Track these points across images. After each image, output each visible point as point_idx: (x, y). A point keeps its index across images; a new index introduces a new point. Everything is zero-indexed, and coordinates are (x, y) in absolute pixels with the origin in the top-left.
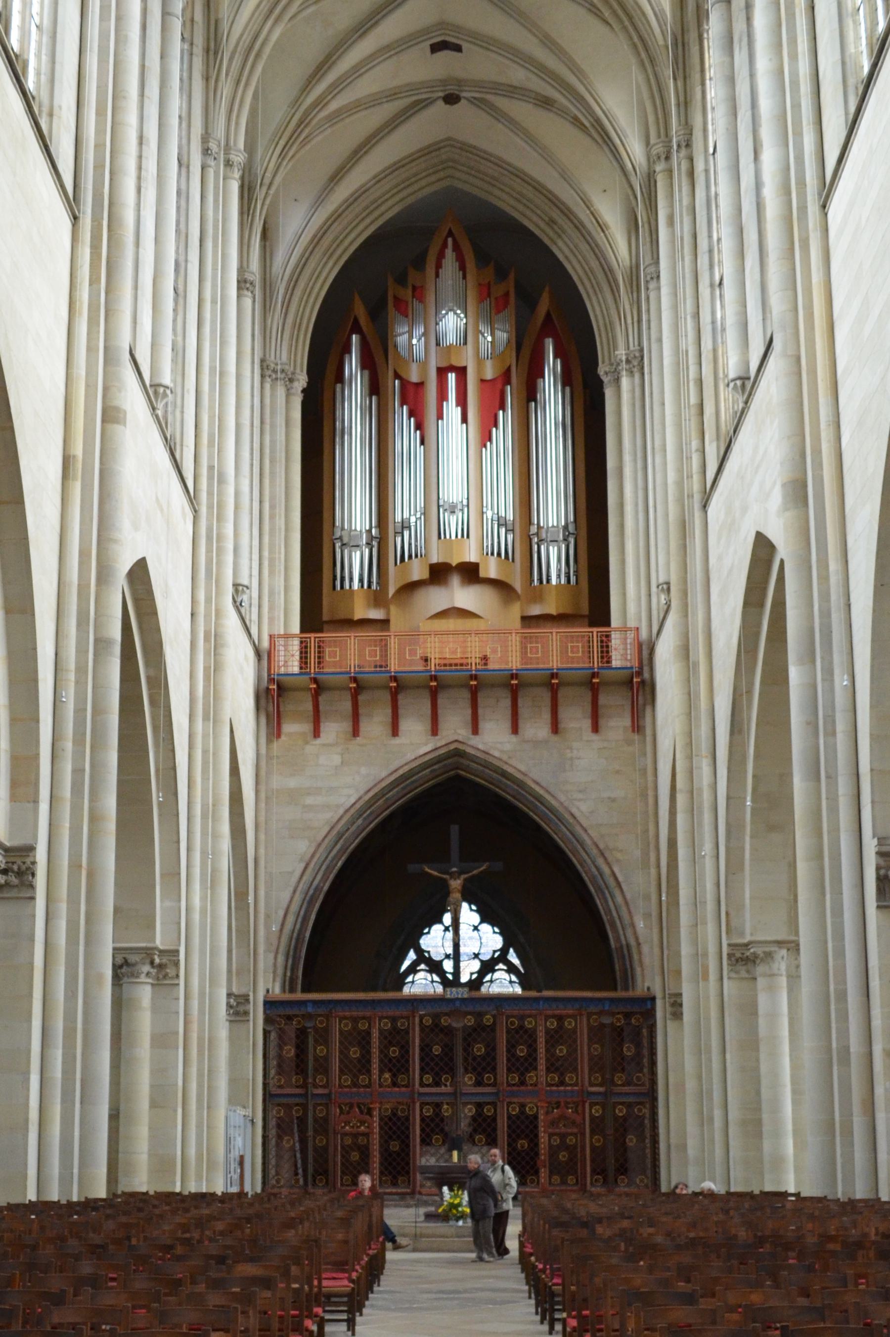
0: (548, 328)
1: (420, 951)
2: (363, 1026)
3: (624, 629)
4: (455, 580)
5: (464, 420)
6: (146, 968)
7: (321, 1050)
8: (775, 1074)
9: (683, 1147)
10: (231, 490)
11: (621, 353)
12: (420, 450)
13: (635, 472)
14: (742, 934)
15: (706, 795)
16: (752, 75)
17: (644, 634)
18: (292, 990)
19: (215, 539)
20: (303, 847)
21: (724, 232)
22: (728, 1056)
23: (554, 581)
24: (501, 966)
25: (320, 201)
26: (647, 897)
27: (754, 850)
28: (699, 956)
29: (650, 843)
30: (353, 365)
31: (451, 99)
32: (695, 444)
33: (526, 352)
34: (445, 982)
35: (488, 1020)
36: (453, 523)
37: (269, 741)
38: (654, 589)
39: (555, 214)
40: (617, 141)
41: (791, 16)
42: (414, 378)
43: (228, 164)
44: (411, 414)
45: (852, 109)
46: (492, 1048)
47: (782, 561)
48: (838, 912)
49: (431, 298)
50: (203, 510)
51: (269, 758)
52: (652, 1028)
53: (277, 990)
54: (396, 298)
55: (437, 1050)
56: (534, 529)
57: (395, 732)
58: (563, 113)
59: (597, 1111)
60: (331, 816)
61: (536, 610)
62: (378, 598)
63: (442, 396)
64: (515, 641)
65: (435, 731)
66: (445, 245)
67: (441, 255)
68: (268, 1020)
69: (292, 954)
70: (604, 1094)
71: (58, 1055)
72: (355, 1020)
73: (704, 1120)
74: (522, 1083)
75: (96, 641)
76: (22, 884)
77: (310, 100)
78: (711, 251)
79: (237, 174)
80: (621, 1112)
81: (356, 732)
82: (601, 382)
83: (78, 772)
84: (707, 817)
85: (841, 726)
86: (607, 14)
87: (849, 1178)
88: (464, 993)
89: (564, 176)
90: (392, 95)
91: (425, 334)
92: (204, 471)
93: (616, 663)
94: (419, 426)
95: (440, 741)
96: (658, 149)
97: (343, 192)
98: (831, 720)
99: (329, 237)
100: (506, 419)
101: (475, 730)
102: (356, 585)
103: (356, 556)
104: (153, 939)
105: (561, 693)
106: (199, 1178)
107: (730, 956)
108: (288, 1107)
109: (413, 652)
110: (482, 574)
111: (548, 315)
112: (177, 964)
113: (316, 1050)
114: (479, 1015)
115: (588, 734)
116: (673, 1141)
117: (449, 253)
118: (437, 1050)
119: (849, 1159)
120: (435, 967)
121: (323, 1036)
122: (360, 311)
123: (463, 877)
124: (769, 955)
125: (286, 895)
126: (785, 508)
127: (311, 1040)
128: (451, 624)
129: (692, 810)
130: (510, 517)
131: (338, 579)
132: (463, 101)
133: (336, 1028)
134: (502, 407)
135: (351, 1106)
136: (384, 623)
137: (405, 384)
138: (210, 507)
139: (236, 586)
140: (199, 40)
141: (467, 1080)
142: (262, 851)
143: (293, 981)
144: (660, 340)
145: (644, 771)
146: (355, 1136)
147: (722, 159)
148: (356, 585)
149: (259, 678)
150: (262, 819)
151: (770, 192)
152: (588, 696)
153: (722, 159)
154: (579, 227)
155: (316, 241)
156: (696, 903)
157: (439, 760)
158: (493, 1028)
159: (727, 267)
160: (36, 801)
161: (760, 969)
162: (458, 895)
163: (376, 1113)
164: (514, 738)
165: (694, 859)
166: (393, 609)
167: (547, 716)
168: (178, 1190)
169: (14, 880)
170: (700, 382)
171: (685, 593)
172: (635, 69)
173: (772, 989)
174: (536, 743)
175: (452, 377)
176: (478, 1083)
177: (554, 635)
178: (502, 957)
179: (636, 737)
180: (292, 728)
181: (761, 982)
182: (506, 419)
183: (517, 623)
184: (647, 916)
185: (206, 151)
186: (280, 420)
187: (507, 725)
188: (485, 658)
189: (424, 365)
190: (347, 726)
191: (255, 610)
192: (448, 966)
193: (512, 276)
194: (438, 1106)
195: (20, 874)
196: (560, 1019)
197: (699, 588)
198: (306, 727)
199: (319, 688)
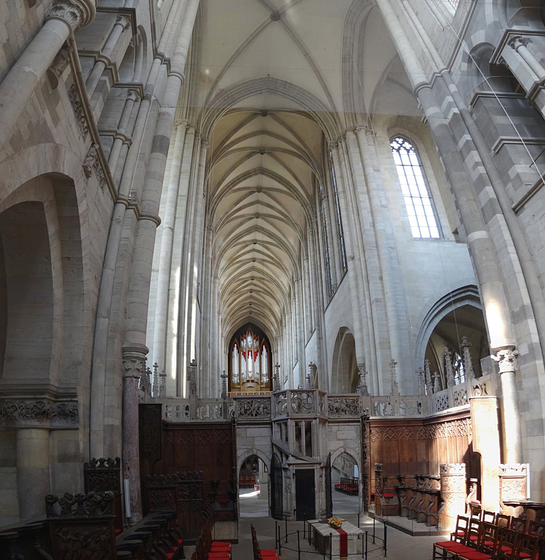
25: (231, 327)
33: (261, 347)
61: (262, 386)
63: (249, 355)
67: (248, 333)
100: (258, 357)
154: (269, 330)
175: (250, 352)
189: (246, 349)
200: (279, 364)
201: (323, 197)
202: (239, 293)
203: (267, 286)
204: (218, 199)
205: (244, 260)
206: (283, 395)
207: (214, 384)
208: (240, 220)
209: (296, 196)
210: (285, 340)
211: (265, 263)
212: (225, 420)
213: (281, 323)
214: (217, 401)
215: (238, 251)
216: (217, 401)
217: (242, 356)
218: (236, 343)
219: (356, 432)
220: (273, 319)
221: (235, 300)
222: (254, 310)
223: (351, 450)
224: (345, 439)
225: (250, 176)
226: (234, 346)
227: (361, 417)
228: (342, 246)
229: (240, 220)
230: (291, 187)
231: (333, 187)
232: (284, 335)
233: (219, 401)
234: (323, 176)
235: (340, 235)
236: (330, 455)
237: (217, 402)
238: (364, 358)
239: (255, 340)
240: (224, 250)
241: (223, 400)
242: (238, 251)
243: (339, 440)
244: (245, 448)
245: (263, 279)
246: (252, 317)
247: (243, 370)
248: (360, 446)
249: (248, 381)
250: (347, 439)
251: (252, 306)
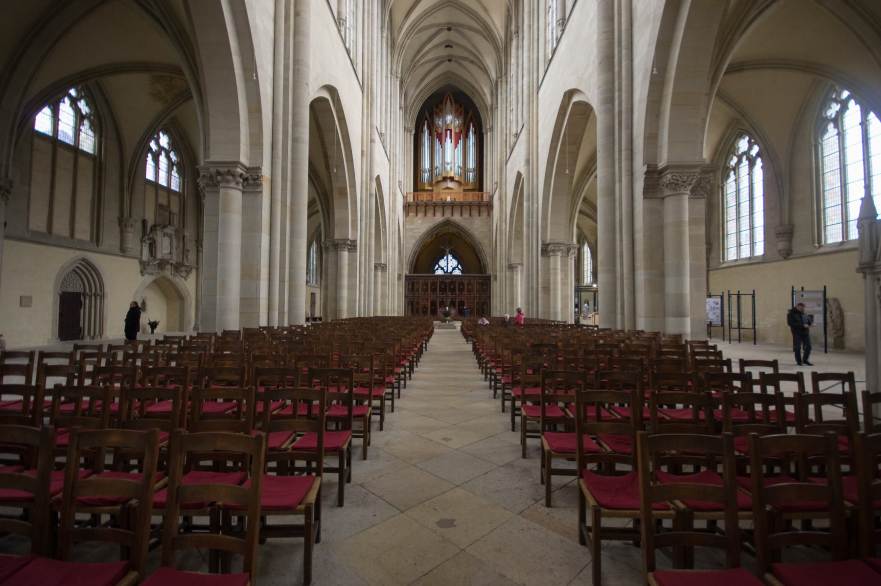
0: (471, 120)
1: (439, 265)
2: (427, 281)
3: (487, 193)
4: (449, 181)
5: (451, 142)
6: (380, 268)
7: (417, 286)
8: (517, 292)
9: (496, 308)
10: (398, 159)
11: (488, 126)
12: (441, 149)
13: (490, 155)
14: (511, 262)
15: (504, 231)
16: (523, 57)
17: (491, 194)
18: (411, 273)
19: (394, 170)
20: (414, 241)
21: (514, 97)
22: (507, 289)
23: (471, 181)
24: (457, 268)
25: (418, 86)
26: (490, 254)
27: (514, 243)
28: (501, 267)
29: (491, 241)
30: (425, 128)
31: (450, 60)
32: (504, 149)
33: (466, 125)
34: (444, 272)
35: (454, 280)
36: (448, 167)
37: (406, 217)
38: (494, 183)
40: (489, 72)
41: (533, 42)
42: (440, 132)
43: (397, 77)
44: (439, 141)
45: (546, 67)
46: (455, 287)
47: (523, 178)
48: (532, 257)
49: (444, 112)
50: (392, 163)
51: (406, 221)
52: (490, 283)
53: (408, 273)
54: (436, 112)
55: (443, 287)
56: (466, 169)
57: (434, 215)
58: (476, 65)
59: (478, 300)
60: (420, 234)
61: (467, 188)
62: (431, 184)
63: (446, 136)
64: (462, 195)
65: (443, 215)
66: (447, 99)
68: (406, 280)
69: (411, 265)
70: (479, 297)
71: (362, 286)
72: (425, 280)
73: (501, 302)
74: (461, 294)
75: (370, 194)
76: (354, 249)
77: (416, 60)
78: (510, 102)
79: (399, 80)
80: (483, 300)
81: (425, 215)
83: (366, 224)
84: (504, 236)
85: (535, 216)
86: (488, 38)
87: (532, 314)
88: (449, 274)
89: (476, 81)
90: (436, 59)
91: (442, 121)
92: (392, 154)
93: (485, 200)
95: (445, 218)
96: (499, 75)
97: (423, 84)
98: (533, 214)
99: (420, 95)
100: (461, 142)
101: (452, 215)
102: (426, 181)
103: (426, 174)
104: (381, 261)
105: (472, 207)
106: (391, 313)
107: (508, 267)
108: (410, 299)
109: (439, 197)
110: (455, 179)
111: (471, 117)
112: (386, 267)
113: (416, 287)
114: (452, 279)
115: (478, 217)
116: (494, 307)
117: (448, 101)
118: (443, 287)
119: (532, 310)
120: (442, 269)
121: (418, 283)
122: (427, 115)
123: (449, 248)
124: (517, 267)
125: (410, 252)
126: (525, 166)
127: (415, 285)
128: (447, 191)
129: (501, 234)
130: (461, 166)
131: (422, 180)
132: (453, 61)
133: (421, 282)
134: (460, 139)
135: (424, 299)
136: (432, 191)
137: (437, 133)
138: (393, 162)
139: (399, 181)
140: (389, 44)
141: (449, 294)
142: (404, 242)
143: (411, 271)
144: (497, 124)
145: (490, 226)
146: (425, 305)
147: (514, 79)
148: (426, 181)
149: (404, 203)
150: (404, 235)
151: (525, 88)
152: (478, 208)
153: (514, 79)
154: (479, 94)
155: (417, 97)
156: (501, 255)
157: (445, 222)
158: (455, 282)
159: (514, 106)
160: (357, 230)
161: (514, 270)
162: (448, 253)
163: (429, 300)
164: (461, 218)
165: (501, 245)
166: (434, 188)
167: (468, 212)
168: (387, 315)
169: (352, 248)
170: (506, 134)
171: (501, 184)
172: (494, 54)
173: (517, 274)
174: (466, 219)
175: (448, 132)
176: (452, 294)
177: (471, 194)
178: (457, 267)
179: (489, 218)
180: (411, 214)
181: (515, 273)
182: (461, 142)
183: (462, 191)
184: (490, 258)
185: (391, 74)
186: (409, 141)
187: (459, 214)
188: (455, 199)
190: (424, 214)
191: (403, 187)
192: (445, 268)
193: (463, 107)
194: (443, 299)
195: (354, 246)
196: (470, 280)
197: (504, 183)
198: (415, 214)
199: (417, 205)
213: (503, 52)
247: (438, 162)
249: (445, 179)
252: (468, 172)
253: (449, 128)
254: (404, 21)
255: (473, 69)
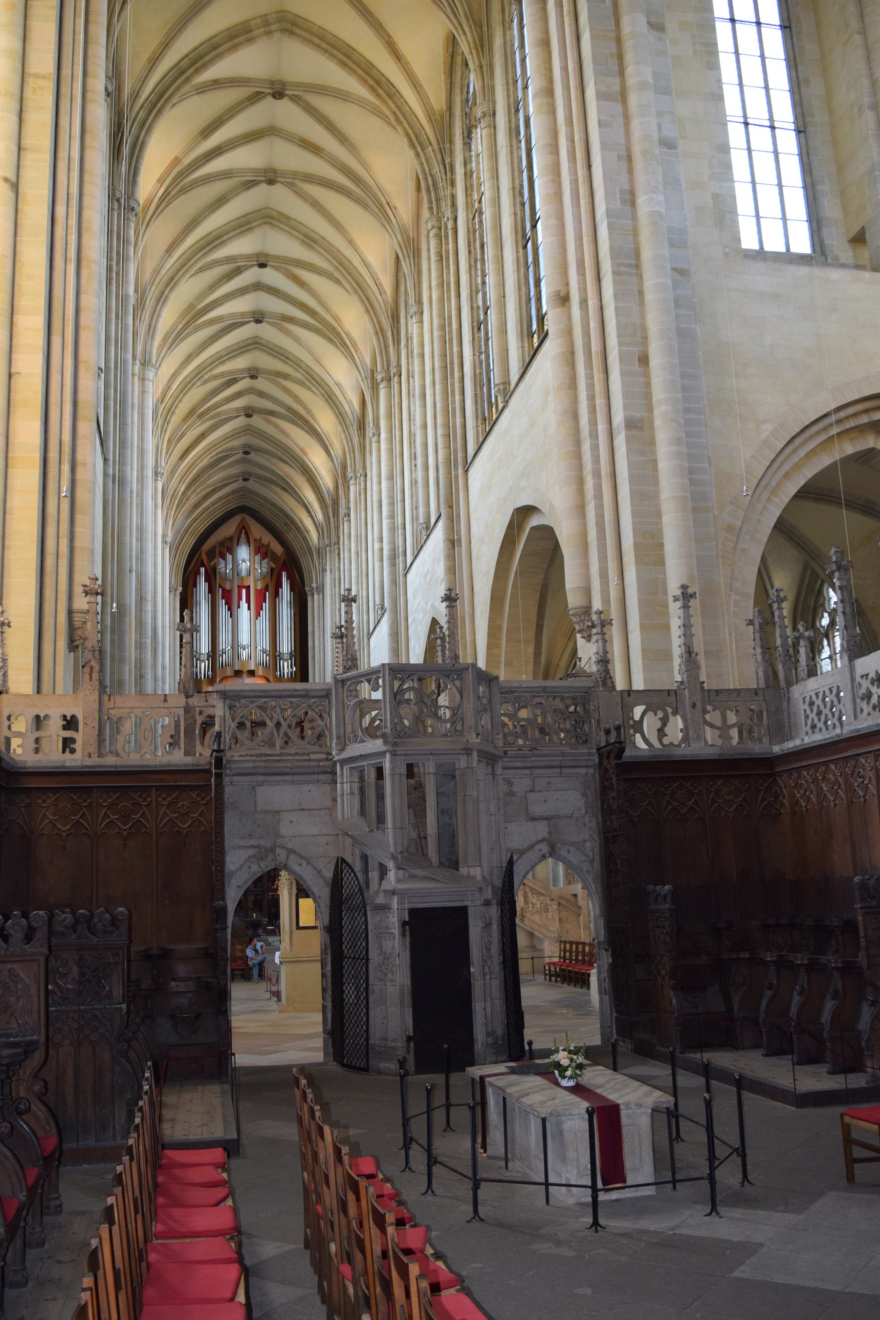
5: (249, 608)
33: (275, 577)
39: (288, 522)
42: (228, 588)
56: (278, 653)
63: (240, 598)
82: (306, 594)
94: (230, 609)
100: (266, 606)
103: (203, 665)
117: (243, 535)
154: (298, 528)
155: (187, 530)
175: (244, 591)
182: (266, 606)
189: (232, 581)
200: (353, 593)
201: (479, 115)
202: (213, 417)
203: (296, 398)
204: (151, 111)
205: (232, 315)
206: (369, 681)
207: (141, 677)
208: (220, 187)
209: (394, 113)
210: (345, 554)
211: (291, 327)
212: (189, 760)
214: (165, 700)
215: (213, 287)
216: (165, 700)
217: (222, 603)
218: (203, 565)
219: (584, 795)
220: (310, 496)
221: (202, 436)
222: (257, 471)
223: (572, 849)
224: (553, 817)
225: (250, 40)
226: (198, 573)
227: (598, 750)
228: (531, 269)
229: (220, 187)
230: (378, 83)
231: (511, 82)
232: (344, 539)
233: (171, 703)
234: (483, 45)
235: (524, 235)
236: (511, 863)
237: (166, 705)
238: (587, 591)
239: (258, 558)
240: (171, 282)
241: (182, 701)
242: (213, 287)
243: (534, 819)
244: (252, 847)
245: (286, 376)
246: (251, 491)
248: (596, 837)
250: (558, 817)
251: (253, 456)
252: (280, 659)
253: (246, 584)
254: (178, 463)
255: (286, 496)
